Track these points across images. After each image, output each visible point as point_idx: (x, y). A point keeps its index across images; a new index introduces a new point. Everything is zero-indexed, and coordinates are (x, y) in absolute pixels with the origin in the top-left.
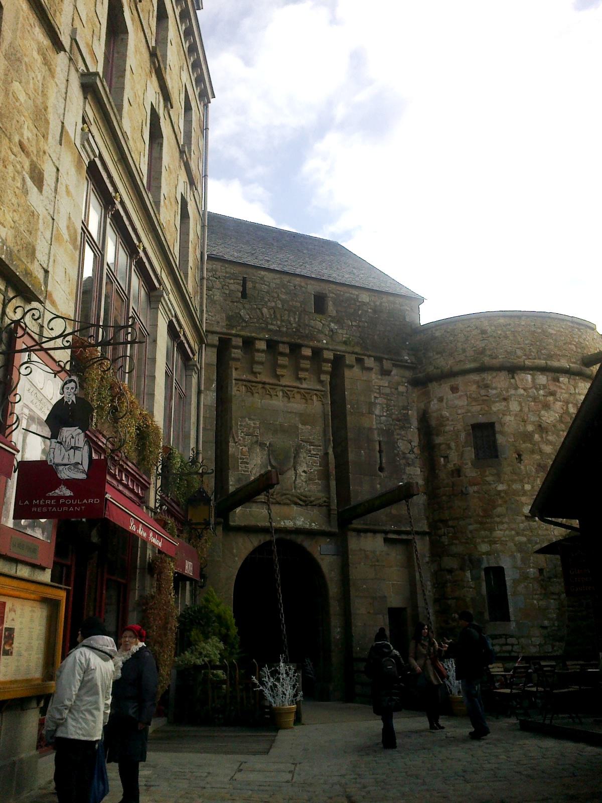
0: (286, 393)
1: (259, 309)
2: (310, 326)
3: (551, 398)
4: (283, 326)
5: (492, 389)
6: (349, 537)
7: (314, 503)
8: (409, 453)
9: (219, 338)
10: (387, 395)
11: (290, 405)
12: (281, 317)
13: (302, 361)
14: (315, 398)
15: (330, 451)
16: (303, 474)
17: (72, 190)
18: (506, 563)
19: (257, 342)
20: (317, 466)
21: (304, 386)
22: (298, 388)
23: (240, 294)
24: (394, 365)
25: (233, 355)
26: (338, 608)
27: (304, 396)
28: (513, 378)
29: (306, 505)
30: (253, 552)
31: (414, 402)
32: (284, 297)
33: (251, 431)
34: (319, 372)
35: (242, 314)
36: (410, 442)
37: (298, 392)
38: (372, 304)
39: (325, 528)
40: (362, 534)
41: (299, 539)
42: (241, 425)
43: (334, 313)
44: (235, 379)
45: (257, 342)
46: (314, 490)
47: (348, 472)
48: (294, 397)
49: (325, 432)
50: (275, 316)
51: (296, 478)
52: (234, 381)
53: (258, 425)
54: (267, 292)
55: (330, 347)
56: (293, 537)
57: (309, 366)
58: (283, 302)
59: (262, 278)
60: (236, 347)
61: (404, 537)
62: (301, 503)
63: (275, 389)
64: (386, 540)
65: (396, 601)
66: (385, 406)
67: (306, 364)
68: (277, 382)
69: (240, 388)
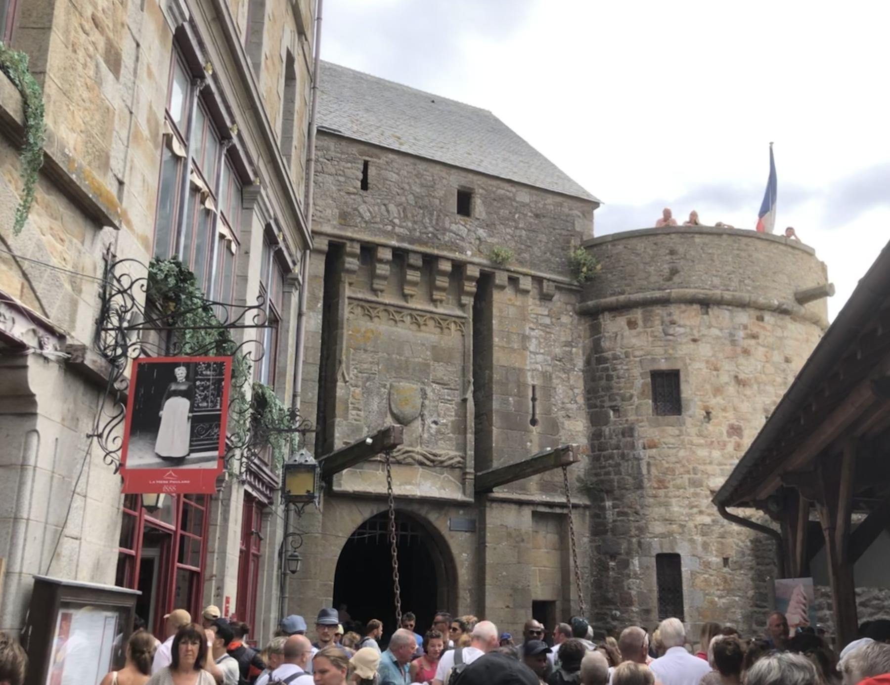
0: (416, 319)
1: (385, 205)
2: (451, 231)
3: (752, 342)
4: (415, 230)
5: (680, 326)
7: (446, 464)
8: (571, 403)
10: (546, 326)
12: (413, 216)
13: (438, 278)
14: (453, 326)
15: (470, 396)
16: (433, 426)
17: (154, 69)
18: (683, 550)
19: (380, 249)
20: (452, 416)
21: (440, 310)
22: (431, 312)
24: (557, 288)
25: (347, 266)
26: (469, 600)
27: (439, 323)
28: (707, 313)
29: (435, 466)
30: (363, 526)
31: (580, 337)
32: (418, 190)
34: (461, 292)
36: (572, 388)
37: (433, 318)
38: (533, 205)
39: (459, 496)
41: (423, 511)
45: (380, 249)
46: (447, 451)
47: (491, 425)
48: (425, 325)
49: (464, 370)
50: (406, 216)
51: (423, 430)
52: (346, 301)
55: (476, 260)
56: (415, 508)
57: (446, 285)
58: (417, 197)
60: (353, 255)
61: (558, 511)
62: (428, 463)
64: (535, 514)
65: (541, 593)
66: (542, 340)
67: (442, 282)
68: (402, 303)
69: (355, 311)
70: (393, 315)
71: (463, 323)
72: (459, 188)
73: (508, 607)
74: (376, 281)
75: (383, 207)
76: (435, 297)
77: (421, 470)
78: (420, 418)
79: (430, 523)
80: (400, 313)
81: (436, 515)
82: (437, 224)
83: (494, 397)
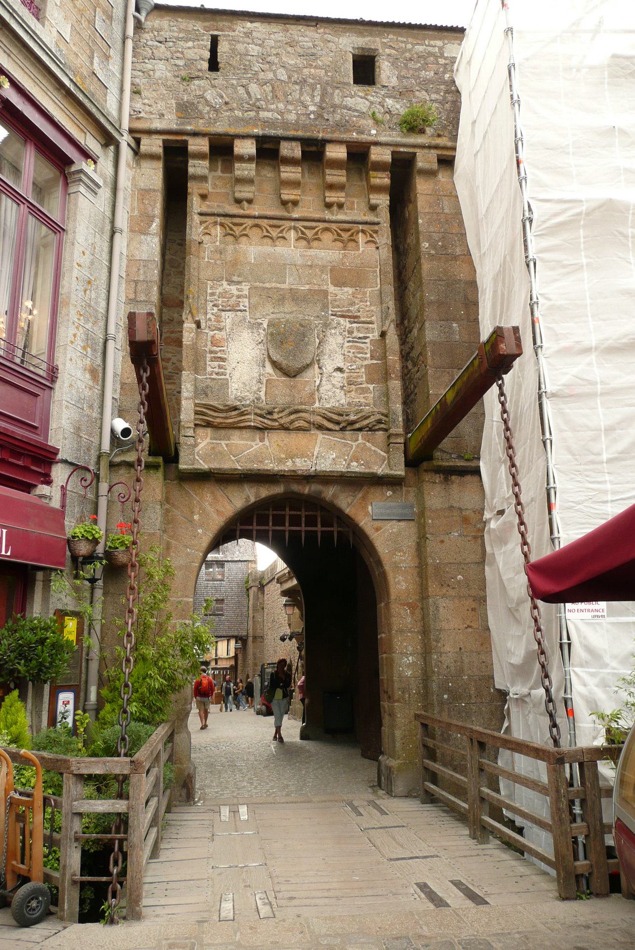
0: (303, 233)
2: (346, 107)
4: (290, 112)
6: (427, 487)
7: (357, 426)
9: (164, 141)
11: (311, 252)
14: (361, 238)
16: (338, 374)
20: (365, 359)
22: (324, 221)
23: (206, 65)
26: (409, 620)
27: (339, 235)
29: (343, 429)
33: (233, 301)
35: (209, 97)
39: (380, 470)
40: (453, 477)
41: (329, 493)
42: (213, 294)
43: (394, 81)
44: (201, 214)
48: (319, 239)
52: (197, 219)
53: (246, 292)
54: (258, 56)
55: (382, 139)
57: (343, 179)
59: (248, 34)
60: (200, 156)
63: (279, 227)
69: (213, 232)
70: (268, 231)
71: (376, 232)
72: (356, 52)
73: (469, 627)
74: (238, 188)
75: (241, 90)
76: (327, 200)
77: (320, 436)
78: (316, 366)
79: (340, 511)
80: (279, 227)
81: (349, 500)
82: (322, 100)
83: (427, 324)
